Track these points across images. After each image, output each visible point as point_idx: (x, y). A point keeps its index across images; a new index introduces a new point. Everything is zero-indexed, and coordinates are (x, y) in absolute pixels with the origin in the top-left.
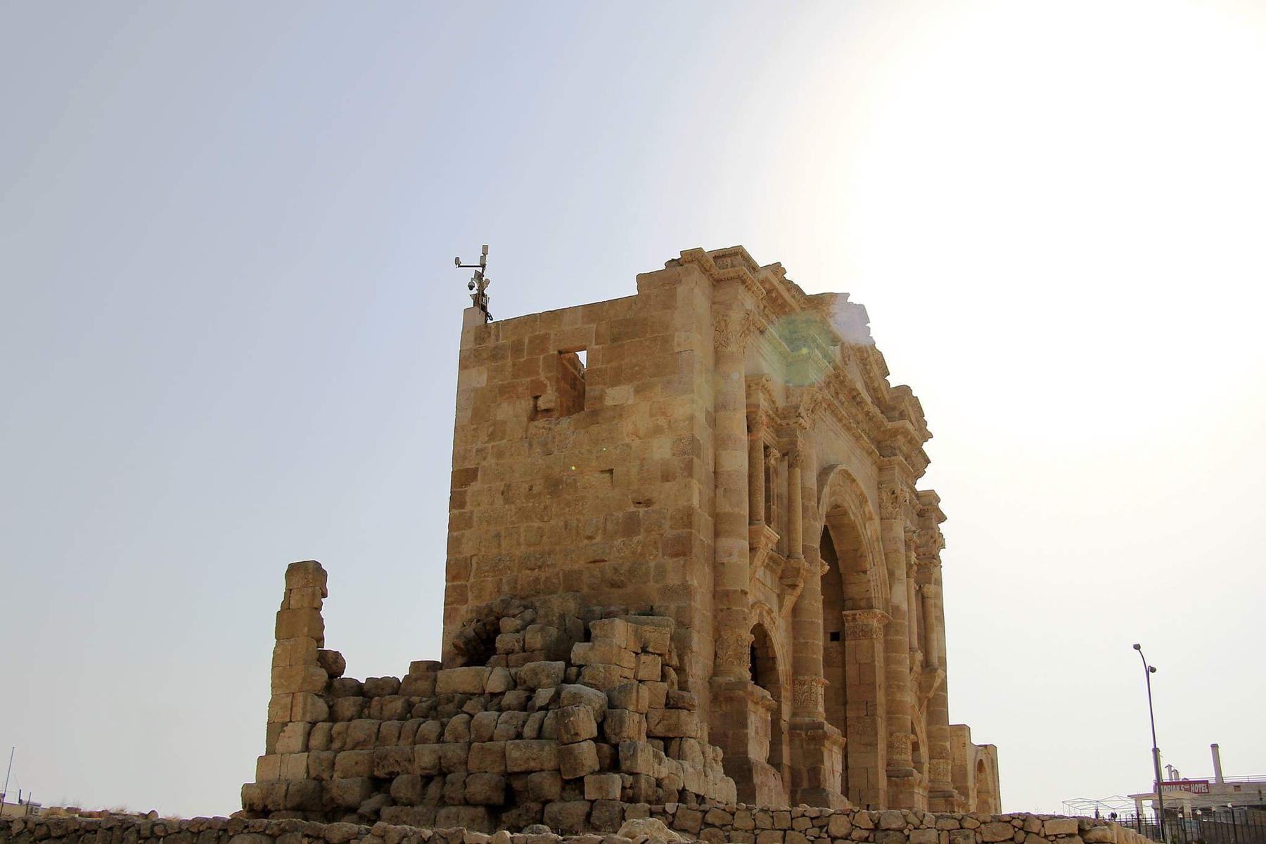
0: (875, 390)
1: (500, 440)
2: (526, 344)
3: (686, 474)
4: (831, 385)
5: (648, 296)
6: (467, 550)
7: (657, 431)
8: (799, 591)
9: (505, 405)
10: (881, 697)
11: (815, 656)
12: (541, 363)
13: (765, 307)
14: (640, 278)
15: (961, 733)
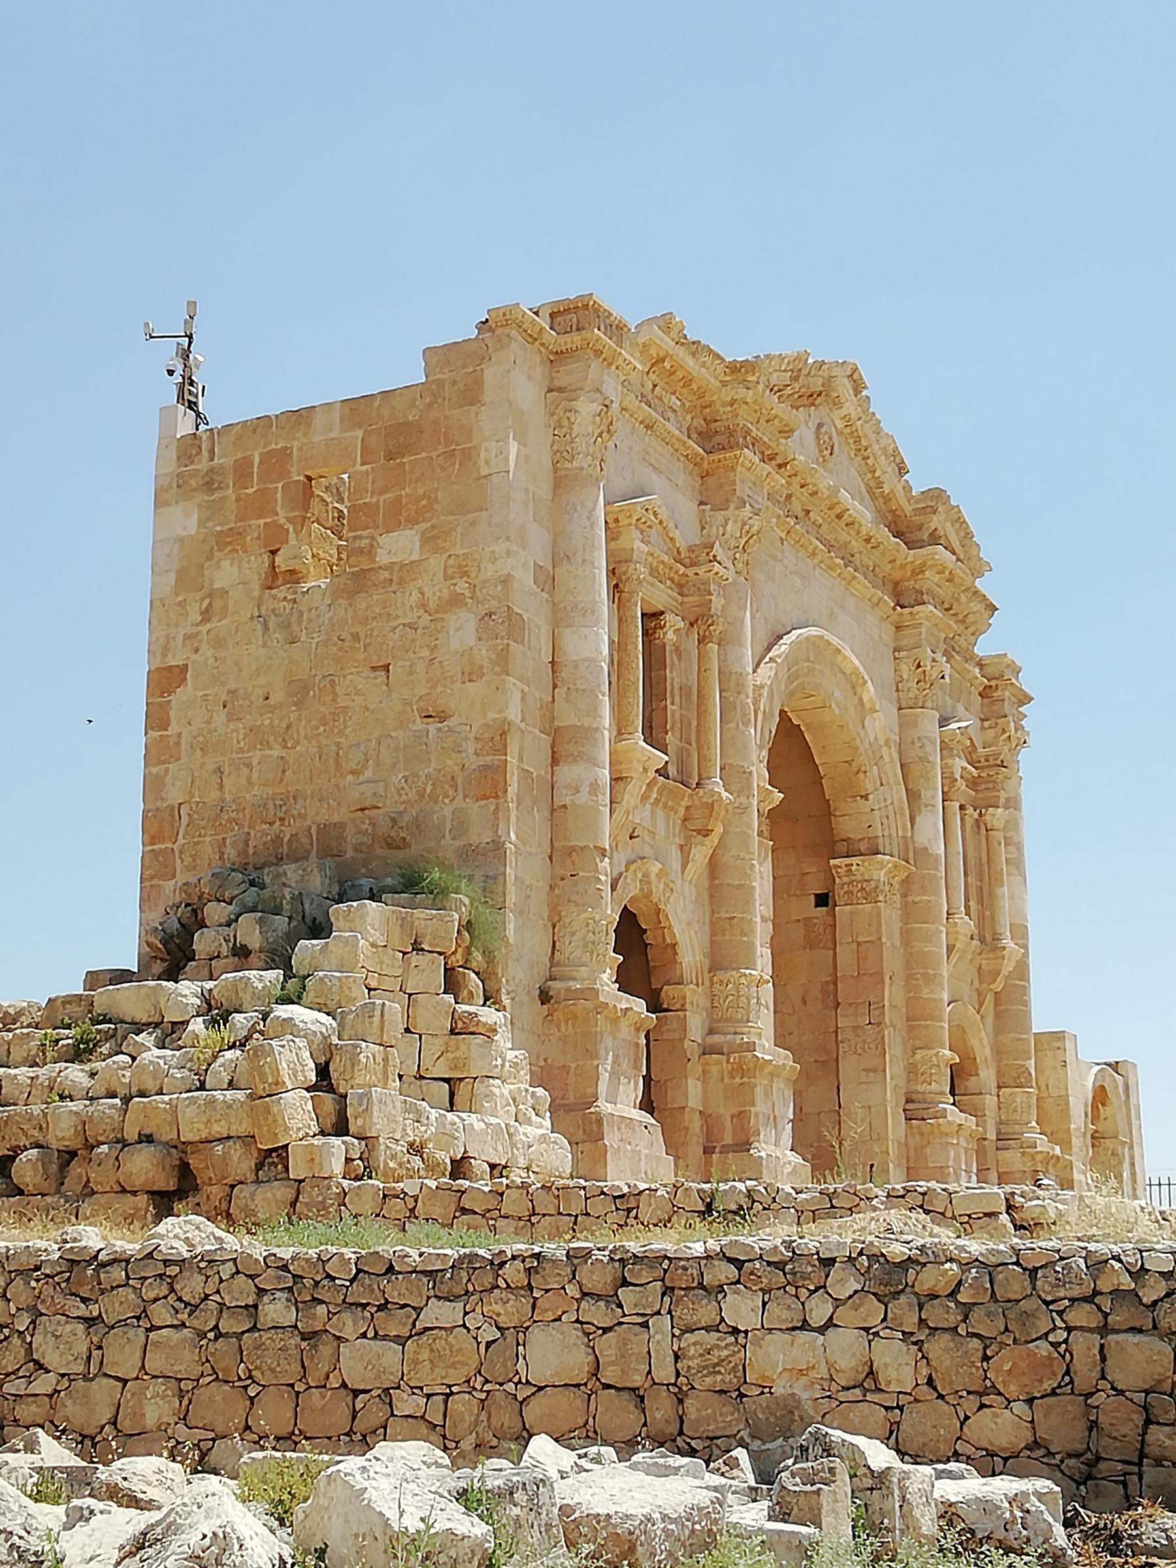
0: (887, 499)
1: (220, 620)
2: (256, 466)
3: (498, 669)
4: (793, 499)
5: (440, 383)
6: (175, 794)
7: (456, 601)
8: (714, 838)
9: (226, 564)
10: (892, 995)
11: (745, 939)
12: (279, 495)
13: (655, 386)
14: (429, 353)
15: (1057, 1044)
